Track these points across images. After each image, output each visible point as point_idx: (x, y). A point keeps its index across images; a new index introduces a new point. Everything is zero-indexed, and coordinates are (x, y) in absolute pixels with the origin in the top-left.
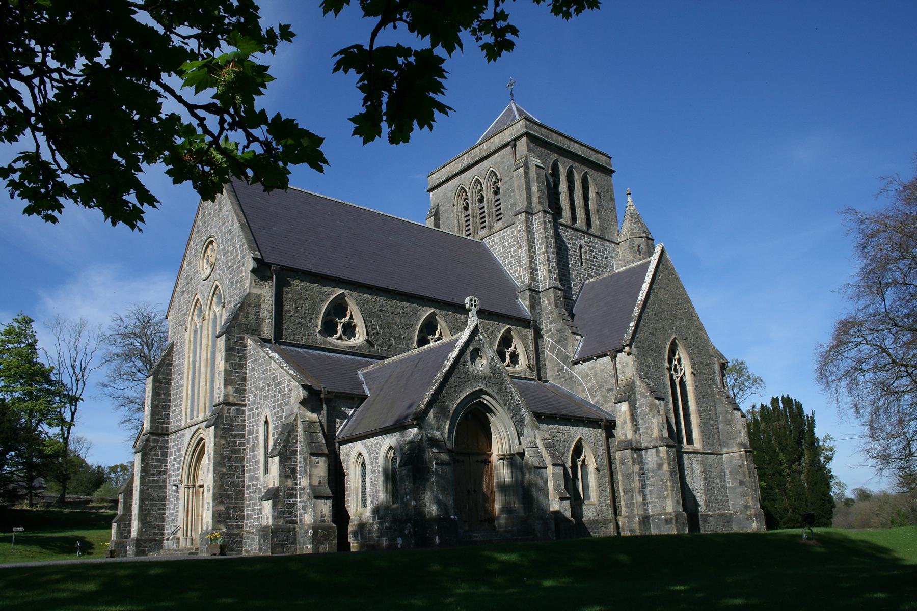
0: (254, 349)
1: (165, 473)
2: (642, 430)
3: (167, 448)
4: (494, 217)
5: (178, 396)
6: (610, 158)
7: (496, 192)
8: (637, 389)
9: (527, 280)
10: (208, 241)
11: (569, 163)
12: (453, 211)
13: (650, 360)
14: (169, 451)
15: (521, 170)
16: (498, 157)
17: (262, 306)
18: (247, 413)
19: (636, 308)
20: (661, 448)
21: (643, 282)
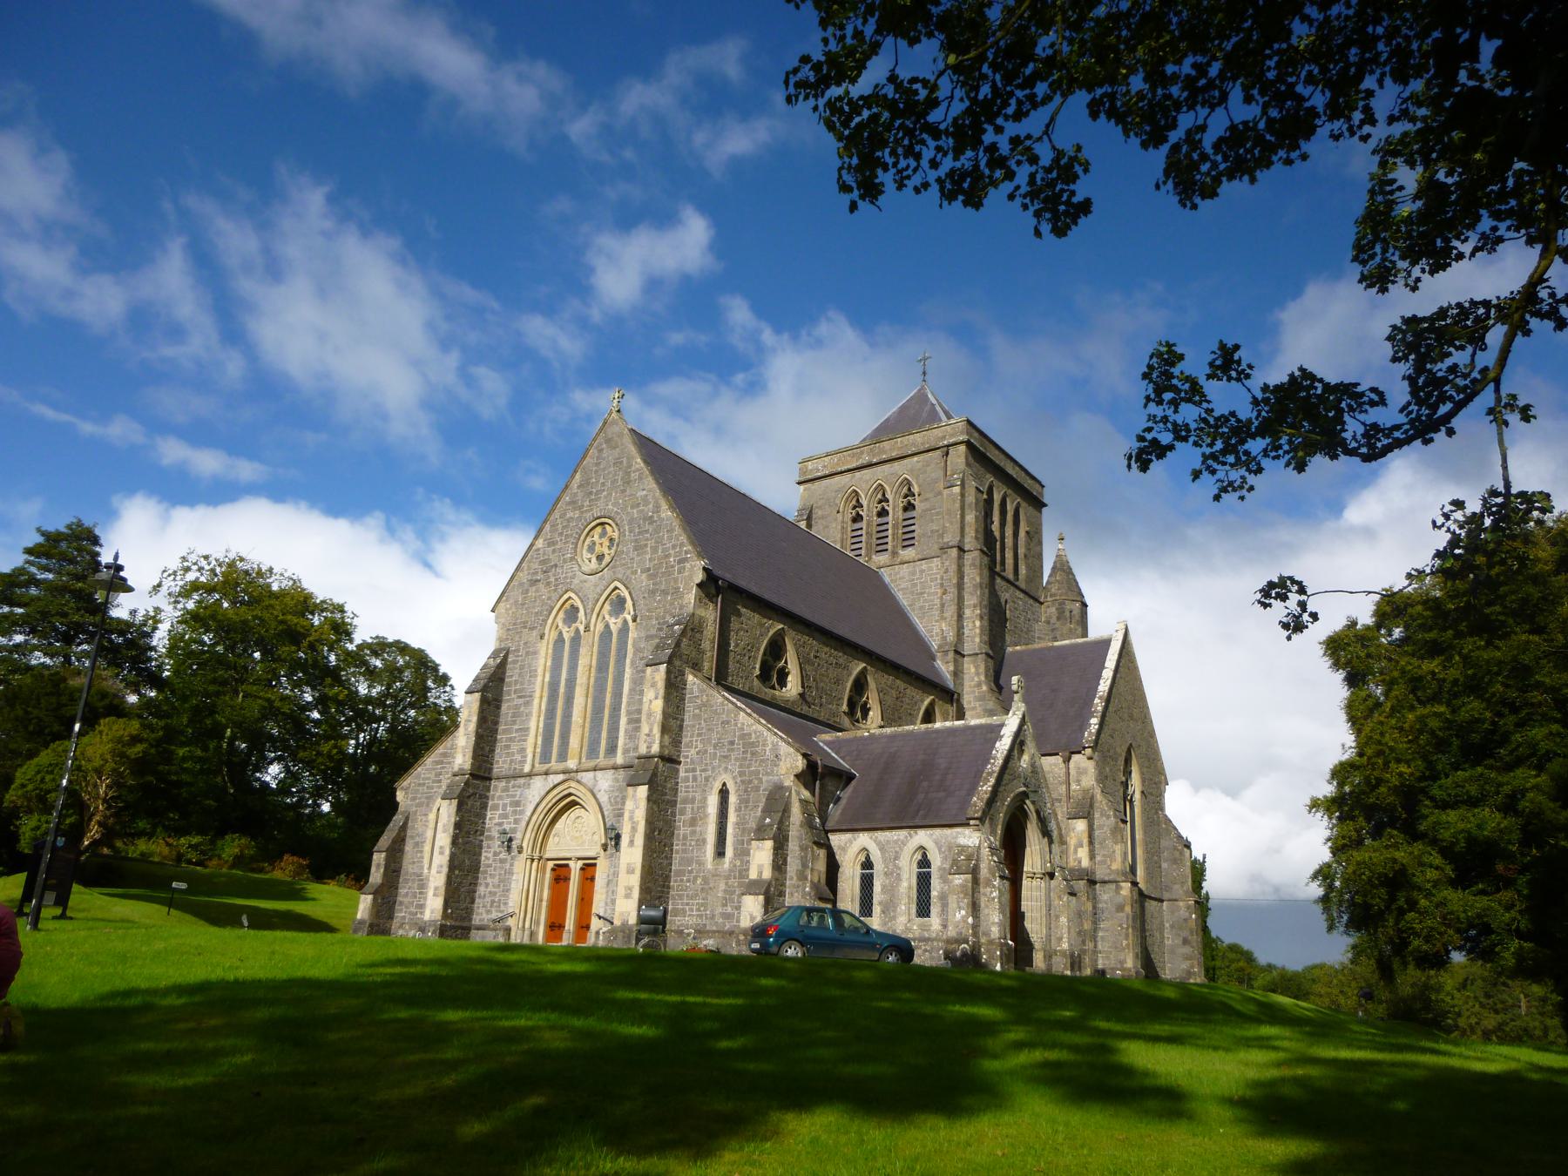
0: (702, 691)
1: (482, 834)
2: (1098, 858)
3: (487, 798)
4: (900, 541)
5: (516, 727)
6: (1043, 486)
7: (909, 507)
8: (1096, 805)
9: (951, 636)
10: (598, 521)
11: (1004, 489)
12: (836, 520)
13: (1107, 769)
14: (490, 803)
15: (957, 490)
16: (918, 462)
17: (705, 632)
18: (682, 774)
19: (1097, 701)
20: (1123, 884)
21: (1103, 667)
